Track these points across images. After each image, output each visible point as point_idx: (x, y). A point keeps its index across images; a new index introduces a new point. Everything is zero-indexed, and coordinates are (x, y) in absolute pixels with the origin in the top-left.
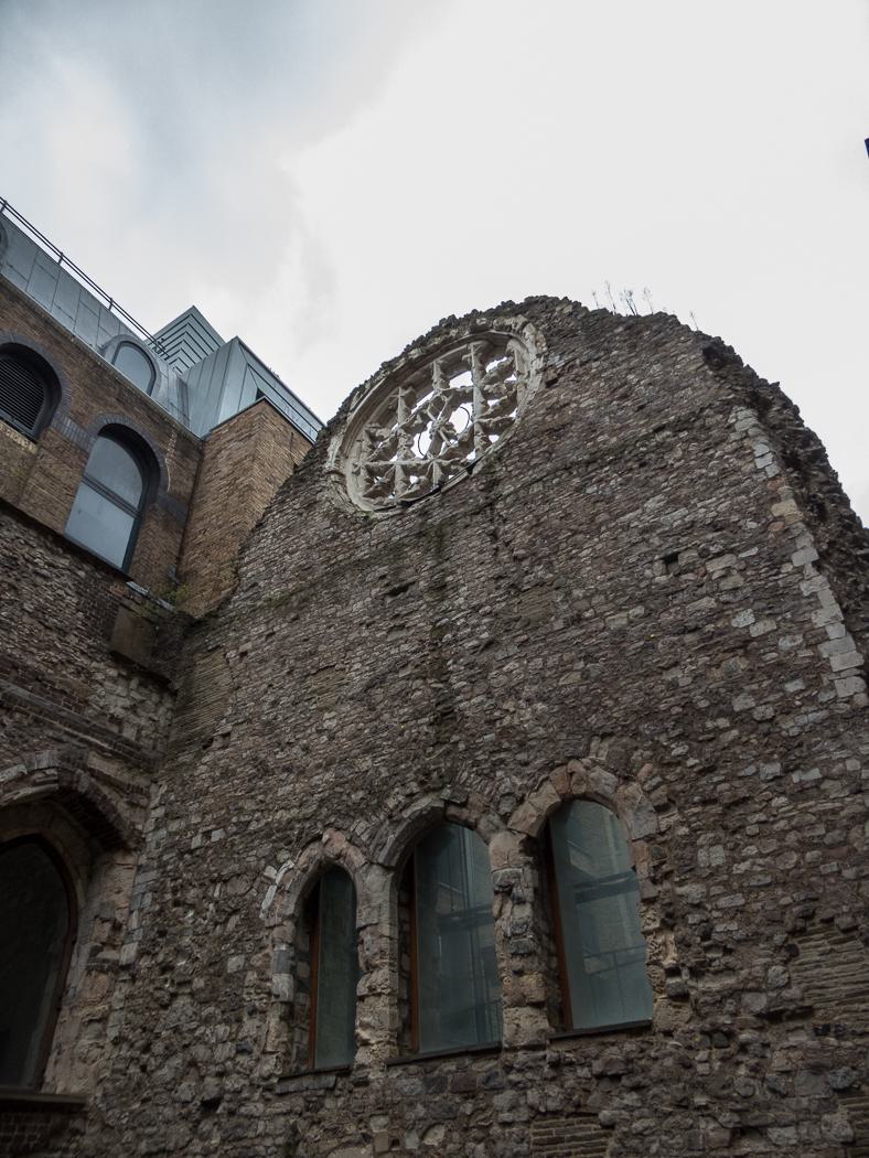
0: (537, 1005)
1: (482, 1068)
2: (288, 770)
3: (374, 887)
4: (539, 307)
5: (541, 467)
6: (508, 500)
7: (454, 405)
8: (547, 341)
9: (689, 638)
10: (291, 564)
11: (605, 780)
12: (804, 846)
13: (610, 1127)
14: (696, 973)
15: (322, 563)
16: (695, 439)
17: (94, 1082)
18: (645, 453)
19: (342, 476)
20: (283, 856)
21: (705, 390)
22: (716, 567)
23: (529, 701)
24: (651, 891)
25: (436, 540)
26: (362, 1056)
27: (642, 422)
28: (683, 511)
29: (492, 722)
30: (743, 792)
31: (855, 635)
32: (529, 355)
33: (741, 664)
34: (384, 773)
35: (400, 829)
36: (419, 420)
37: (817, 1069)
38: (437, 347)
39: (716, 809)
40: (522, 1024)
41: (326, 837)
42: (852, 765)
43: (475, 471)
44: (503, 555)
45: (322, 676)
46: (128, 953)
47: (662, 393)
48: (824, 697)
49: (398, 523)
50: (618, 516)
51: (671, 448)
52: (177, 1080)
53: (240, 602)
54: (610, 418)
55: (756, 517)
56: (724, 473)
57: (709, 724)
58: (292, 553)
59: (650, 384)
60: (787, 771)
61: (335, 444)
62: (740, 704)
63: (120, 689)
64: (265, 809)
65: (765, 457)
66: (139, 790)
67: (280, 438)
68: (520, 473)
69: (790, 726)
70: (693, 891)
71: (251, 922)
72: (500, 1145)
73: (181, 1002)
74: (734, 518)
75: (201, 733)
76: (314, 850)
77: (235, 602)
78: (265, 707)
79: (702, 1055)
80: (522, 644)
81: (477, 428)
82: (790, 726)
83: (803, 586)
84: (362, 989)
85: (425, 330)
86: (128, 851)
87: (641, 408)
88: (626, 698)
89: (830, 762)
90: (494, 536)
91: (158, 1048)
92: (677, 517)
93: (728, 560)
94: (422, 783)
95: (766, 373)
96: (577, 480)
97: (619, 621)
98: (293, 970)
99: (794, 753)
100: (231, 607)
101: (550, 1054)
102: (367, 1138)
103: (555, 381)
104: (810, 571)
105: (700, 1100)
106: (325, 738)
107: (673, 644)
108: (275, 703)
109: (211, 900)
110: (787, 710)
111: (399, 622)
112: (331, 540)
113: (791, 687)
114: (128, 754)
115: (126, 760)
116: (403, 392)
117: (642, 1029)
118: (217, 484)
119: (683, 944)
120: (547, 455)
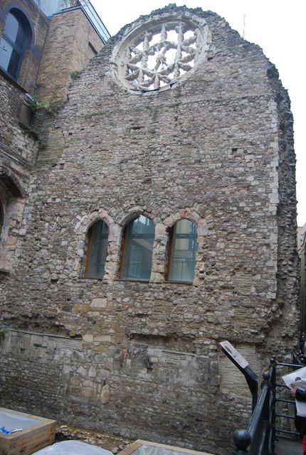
0: (162, 273)
1: (142, 286)
2: (87, 184)
3: (115, 232)
4: (213, 18)
6: (185, 106)
7: (167, 49)
9: (233, 179)
11: (196, 216)
12: (246, 249)
13: (176, 305)
14: (207, 274)
16: (254, 107)
17: (11, 267)
18: (236, 106)
19: (116, 65)
20: (83, 213)
22: (248, 158)
23: (178, 185)
24: (202, 250)
25: (155, 114)
26: (106, 276)
28: (243, 134)
29: (164, 188)
30: (234, 230)
31: (279, 192)
32: (202, 41)
33: (245, 192)
34: (124, 195)
35: (127, 215)
36: (152, 51)
37: (230, 301)
38: (166, 18)
39: (226, 233)
40: (156, 277)
41: (100, 211)
42: (265, 230)
43: (174, 87)
44: (178, 128)
45: (103, 152)
46: (23, 232)
48: (265, 209)
50: (220, 128)
51: (246, 107)
52: (43, 272)
53: (68, 110)
55: (265, 145)
56: (260, 124)
57: (231, 208)
58: (93, 96)
60: (248, 227)
61: (116, 49)
62: (241, 204)
63: (22, 138)
64: (76, 195)
65: (274, 124)
66: (26, 177)
67: (85, 28)
69: (253, 215)
70: (213, 253)
71: (70, 231)
72: (144, 304)
73: (42, 251)
74: (258, 143)
75: (51, 161)
76: (95, 214)
77: (67, 109)
78: (79, 158)
79: (204, 293)
80: (180, 164)
81: (176, 65)
82: (253, 215)
83: (271, 173)
84: (108, 258)
85: (162, 7)
86: (22, 198)
87: (240, 85)
88: (208, 193)
89: (259, 228)
90: (176, 119)
91: (36, 262)
92: (240, 135)
93: (252, 157)
94: (136, 202)
95: (285, 85)
96: (210, 108)
97: (212, 166)
98: (84, 249)
99: (252, 224)
100: (64, 111)
101: (163, 286)
102: (105, 297)
103: (212, 58)
104: (274, 169)
105: (200, 302)
106: (102, 177)
107: (227, 180)
108: (83, 158)
109: (55, 221)
110: (254, 210)
111: (135, 141)
113: (257, 204)
114: (23, 163)
115: (23, 166)
116: (147, 34)
117: (190, 284)
118: (55, 45)
119: (206, 266)
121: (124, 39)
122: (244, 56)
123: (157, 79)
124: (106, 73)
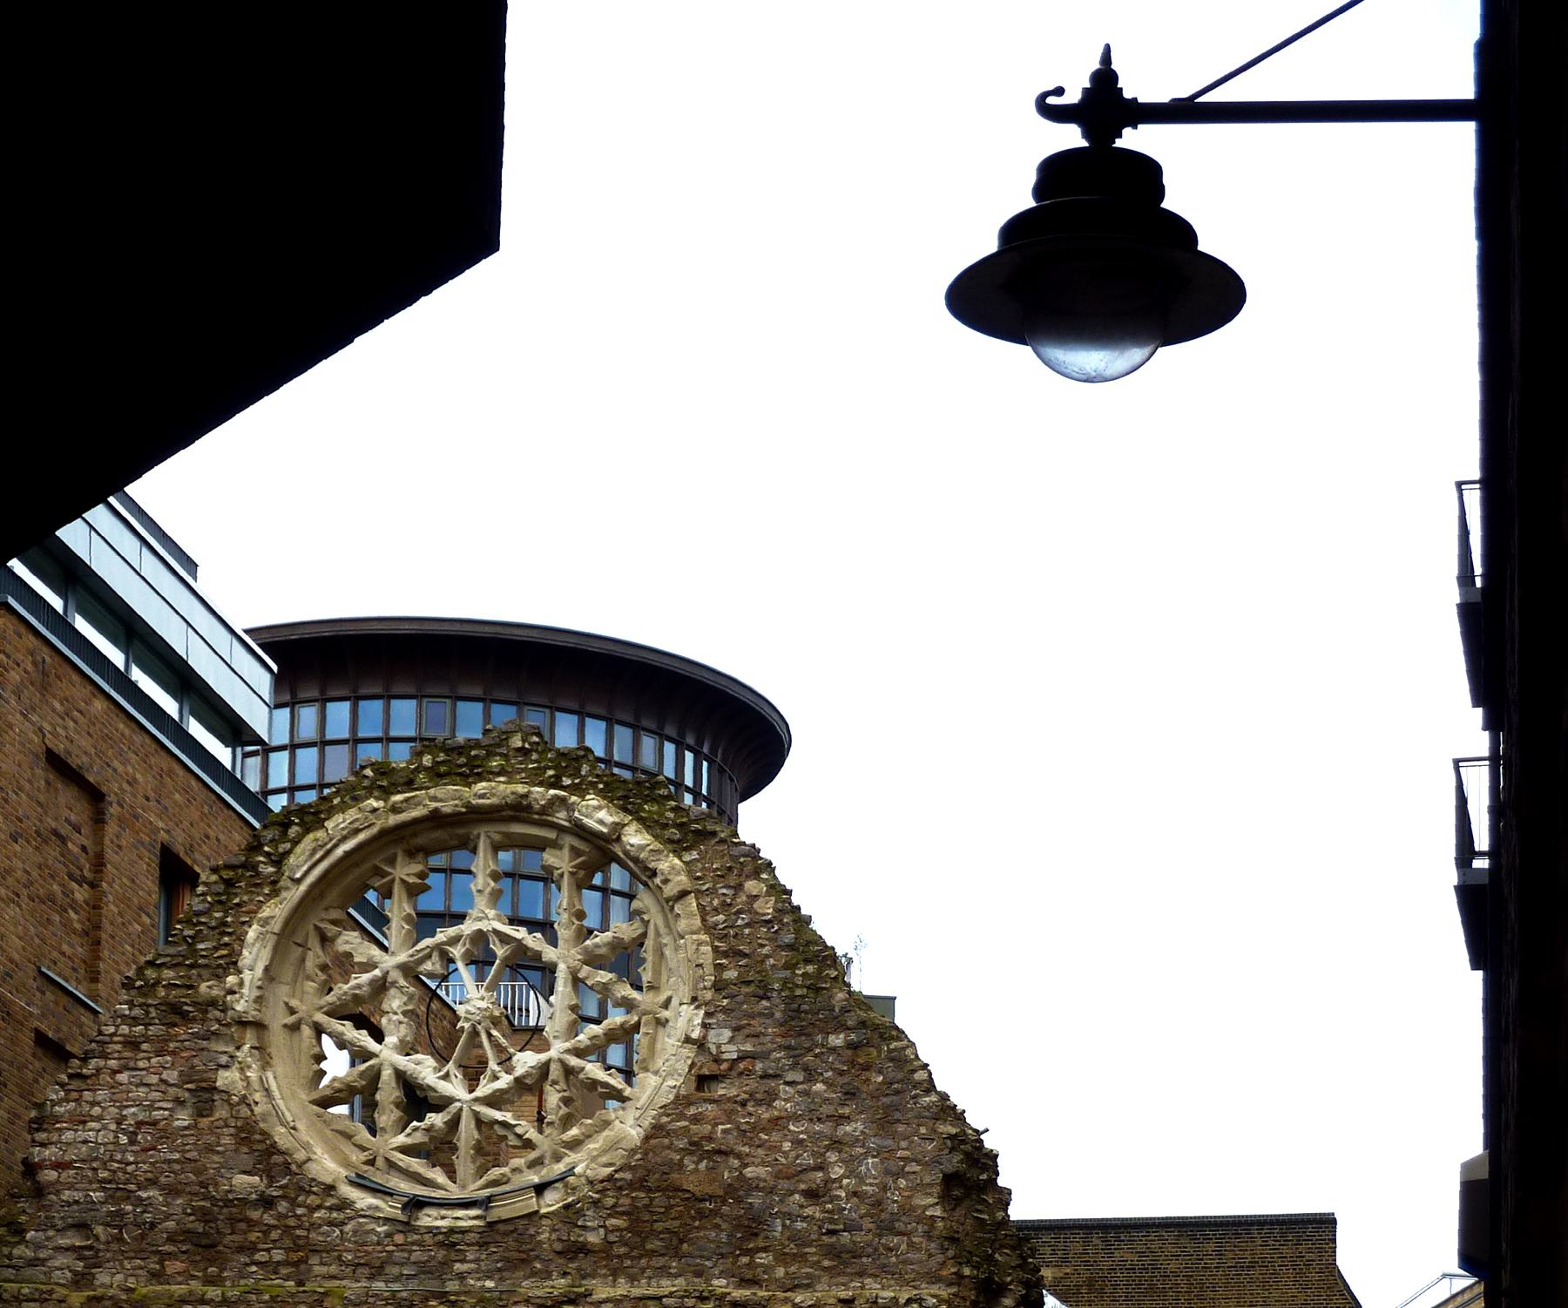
5: (661, 1261)
8: (719, 968)
10: (168, 1217)
15: (240, 1249)
21: (922, 1256)
27: (826, 1263)
47: (867, 1224)
49: (399, 1238)
54: (784, 1226)
58: (172, 1191)
59: (855, 1194)
68: (626, 1256)
103: (714, 1078)
112: (255, 1205)
120: (675, 1242)
121: (294, 895)
122: (850, 1094)
123: (466, 1125)
124: (225, 1078)
